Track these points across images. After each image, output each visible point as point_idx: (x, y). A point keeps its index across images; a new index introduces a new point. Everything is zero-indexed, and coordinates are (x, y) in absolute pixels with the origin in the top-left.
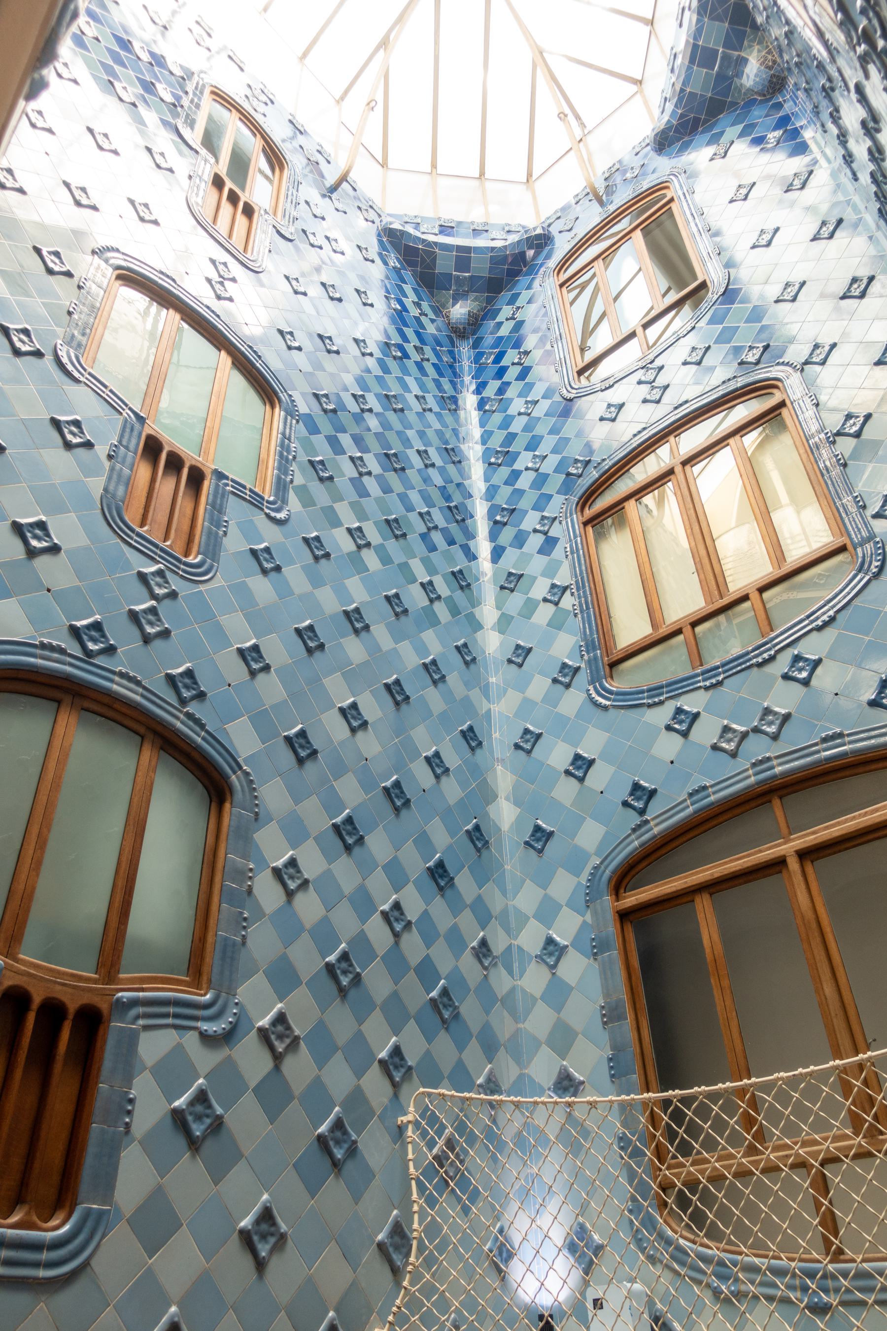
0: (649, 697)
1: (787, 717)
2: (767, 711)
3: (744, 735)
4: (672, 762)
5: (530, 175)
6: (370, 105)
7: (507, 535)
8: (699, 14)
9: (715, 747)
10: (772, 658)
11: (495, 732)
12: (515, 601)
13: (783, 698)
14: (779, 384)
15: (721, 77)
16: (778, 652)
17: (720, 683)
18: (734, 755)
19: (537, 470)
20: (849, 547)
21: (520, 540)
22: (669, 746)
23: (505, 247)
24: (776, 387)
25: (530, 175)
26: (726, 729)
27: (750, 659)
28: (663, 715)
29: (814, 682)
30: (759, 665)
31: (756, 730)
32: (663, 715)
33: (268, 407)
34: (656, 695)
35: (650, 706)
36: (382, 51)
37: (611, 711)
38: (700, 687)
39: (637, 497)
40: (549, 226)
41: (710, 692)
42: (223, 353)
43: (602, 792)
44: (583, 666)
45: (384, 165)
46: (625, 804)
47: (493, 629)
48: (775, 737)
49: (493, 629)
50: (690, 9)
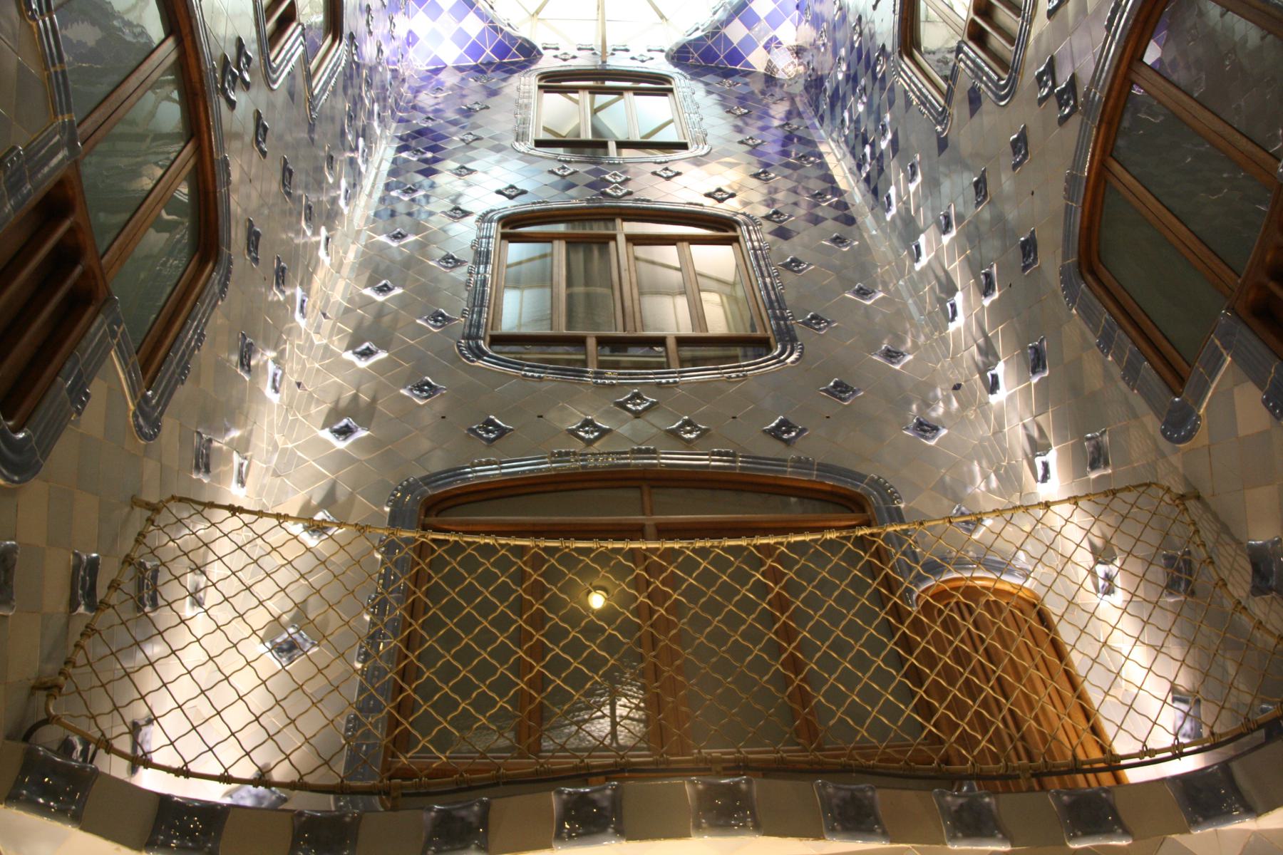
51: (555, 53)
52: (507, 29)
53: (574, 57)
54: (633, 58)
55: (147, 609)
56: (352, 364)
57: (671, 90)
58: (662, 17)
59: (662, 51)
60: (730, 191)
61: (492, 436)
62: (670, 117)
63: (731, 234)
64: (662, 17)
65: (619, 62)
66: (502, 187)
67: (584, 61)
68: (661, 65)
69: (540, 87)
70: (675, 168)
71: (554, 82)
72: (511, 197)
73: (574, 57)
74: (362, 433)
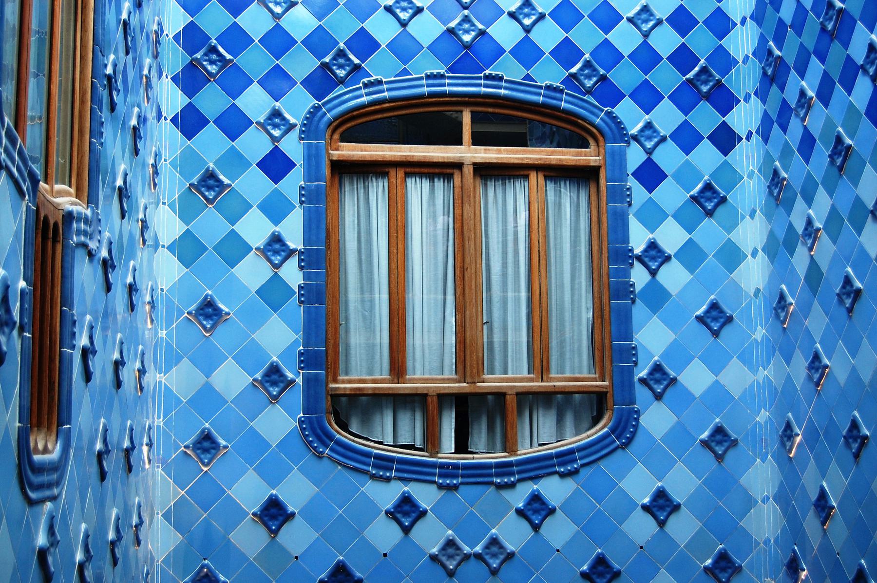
0: (375, 466)
1: (511, 556)
2: (494, 541)
3: (467, 557)
4: (385, 555)
7: (212, 100)
9: (434, 558)
11: (159, 418)
12: (211, 224)
13: (513, 534)
14: (601, 139)
16: (520, 480)
17: (455, 488)
19: (277, 17)
21: (234, 124)
22: (384, 535)
26: (450, 543)
27: (491, 475)
28: (387, 494)
29: (543, 530)
30: (500, 487)
31: (478, 556)
32: (387, 494)
34: (383, 468)
35: (373, 477)
37: (326, 461)
38: (434, 482)
39: (408, 170)
41: (443, 493)
43: (296, 558)
44: (300, 380)
47: (171, 248)
49: (171, 248)
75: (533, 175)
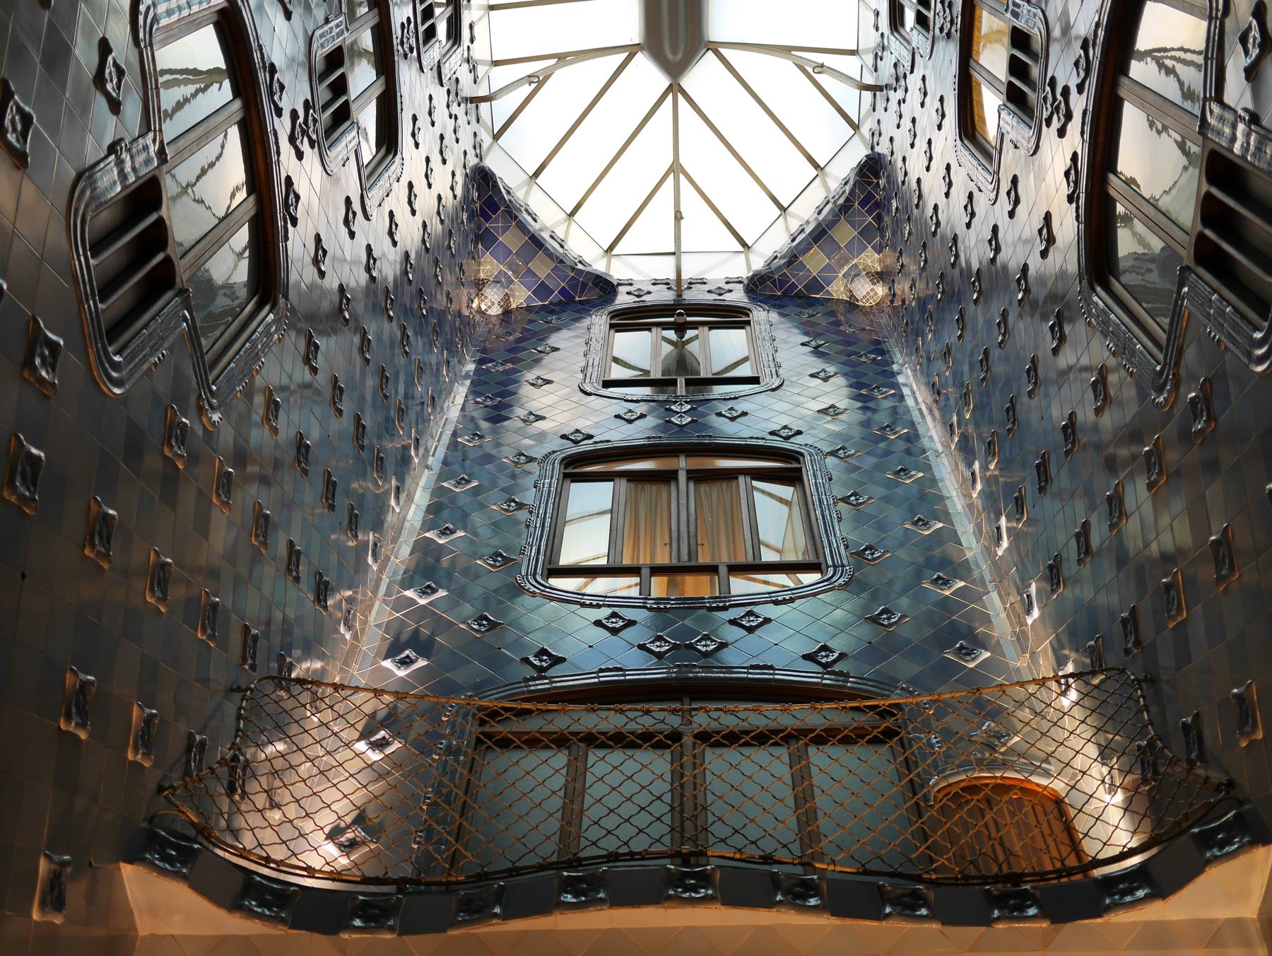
5: (611, 248)
6: (529, 78)
8: (840, 210)
10: (725, 608)
15: (828, 268)
18: (659, 656)
20: (823, 566)
23: (573, 269)
24: (799, 462)
25: (611, 248)
33: (383, 151)
36: (554, 61)
40: (619, 284)
42: (383, 78)
45: (496, 137)
46: (526, 661)
48: (706, 655)
50: (835, 203)
51: (629, 288)
52: (580, 266)
53: (649, 293)
54: (709, 292)
55: (237, 798)
56: (413, 602)
57: (748, 323)
58: (744, 244)
59: (740, 282)
60: (796, 428)
61: (545, 664)
62: (745, 354)
63: (795, 465)
64: (744, 244)
65: (697, 295)
66: (567, 431)
67: (663, 296)
68: (737, 296)
69: (612, 326)
70: (740, 406)
71: (630, 319)
72: (576, 442)
73: (649, 293)
74: (422, 663)
75: (741, 479)
